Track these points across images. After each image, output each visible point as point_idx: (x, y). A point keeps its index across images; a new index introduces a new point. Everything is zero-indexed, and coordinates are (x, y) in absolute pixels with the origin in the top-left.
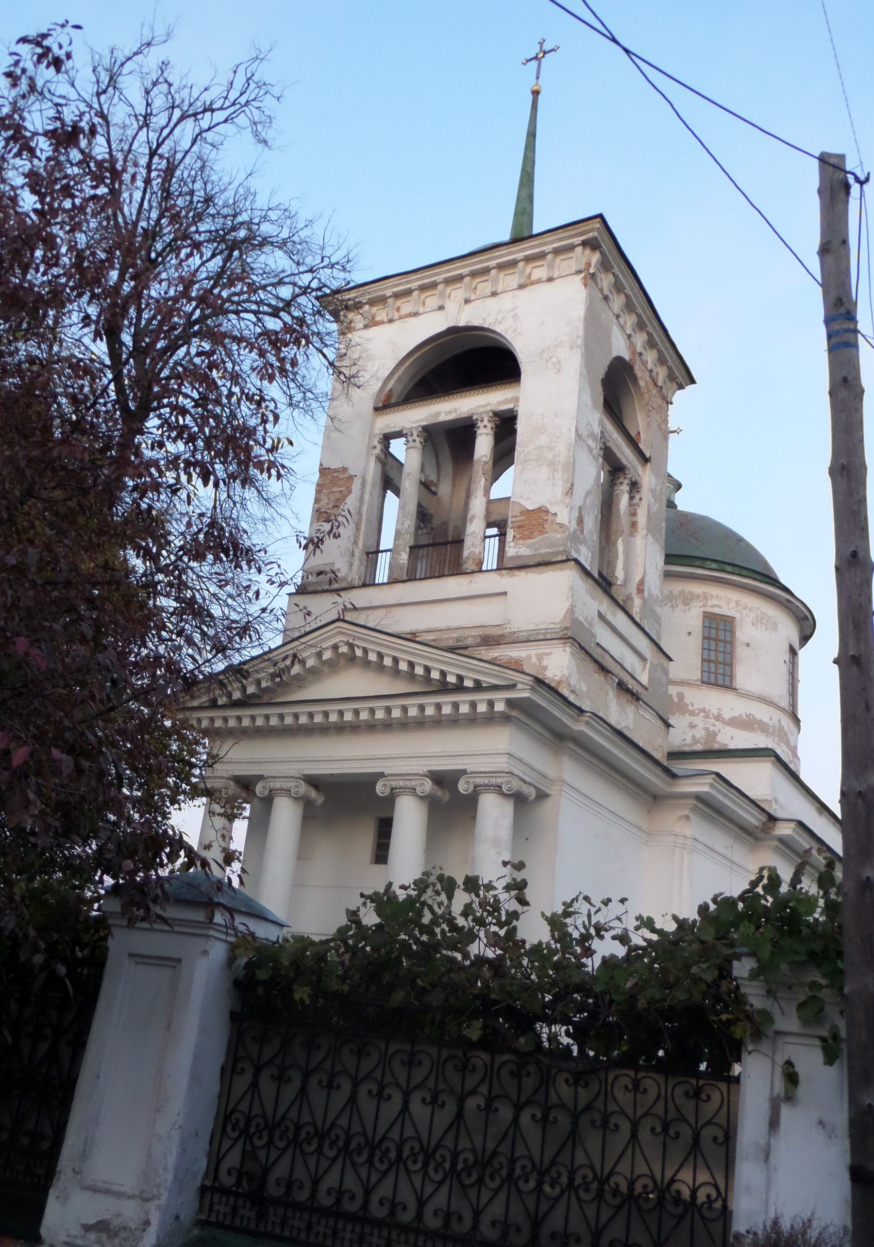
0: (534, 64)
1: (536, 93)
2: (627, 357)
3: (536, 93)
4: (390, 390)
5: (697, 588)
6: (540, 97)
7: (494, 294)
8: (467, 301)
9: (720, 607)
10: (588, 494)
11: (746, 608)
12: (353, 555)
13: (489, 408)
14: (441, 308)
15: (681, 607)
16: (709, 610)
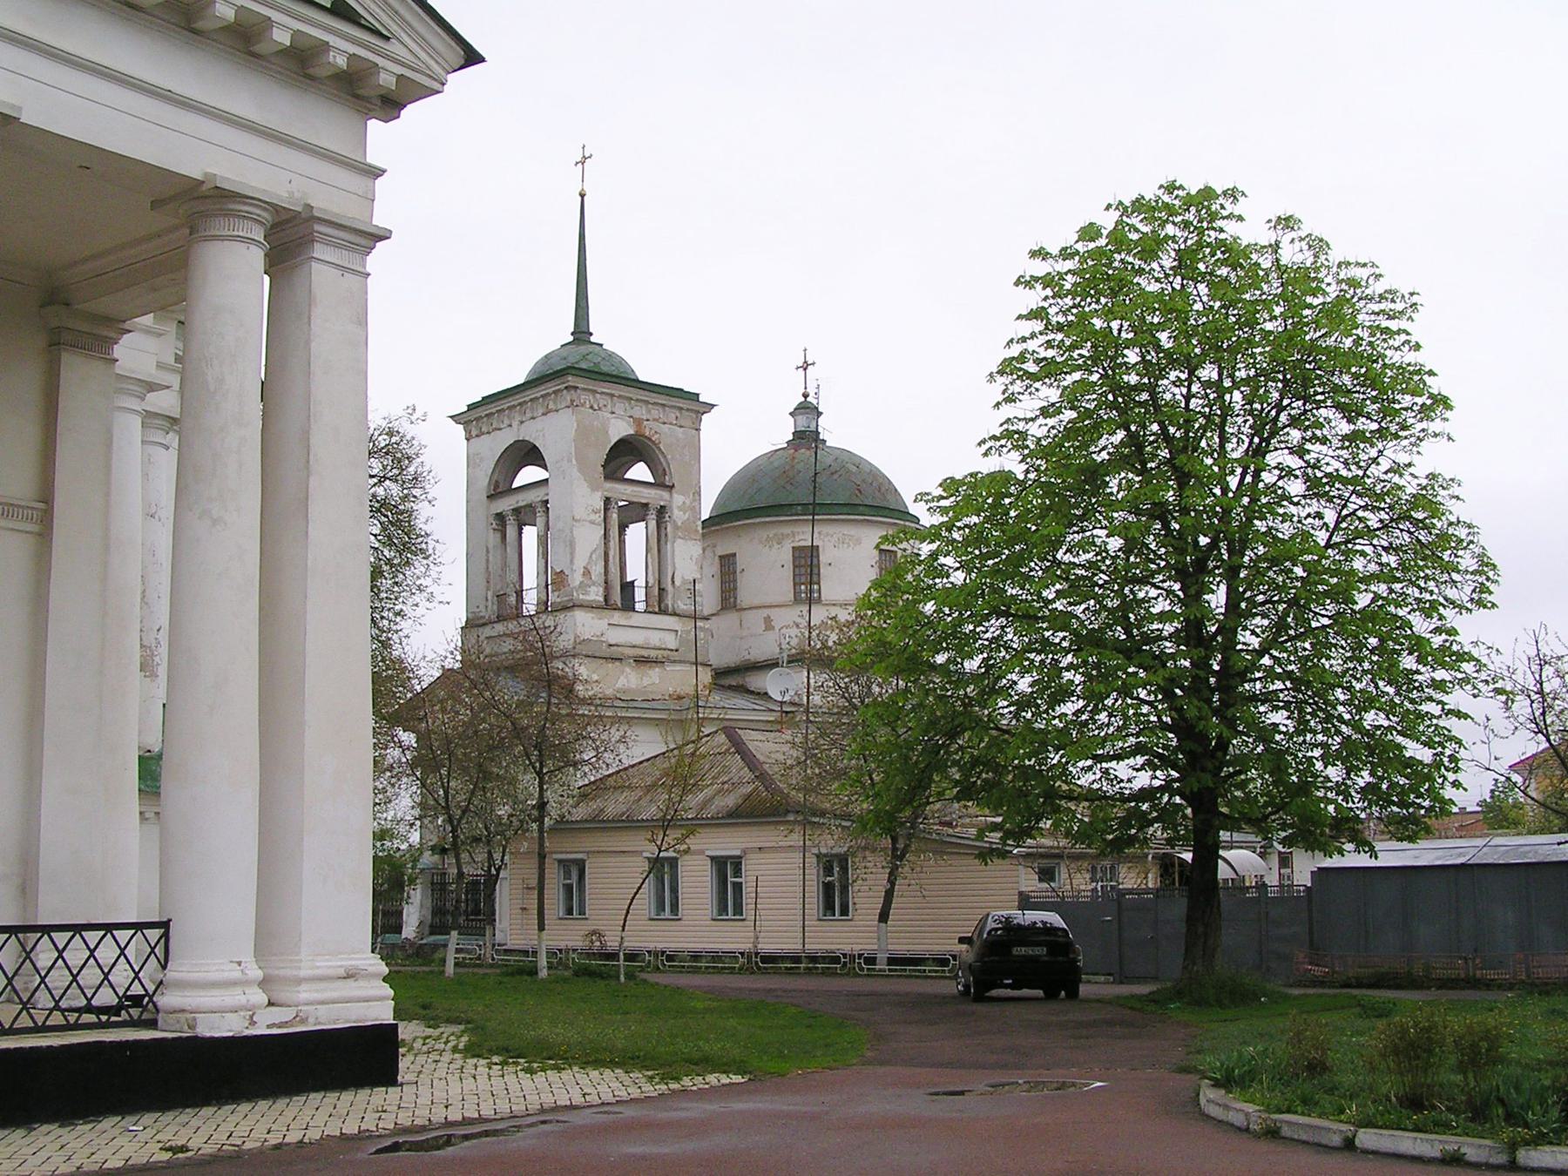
0: (580, 165)
1: (582, 196)
3: (582, 196)
4: (497, 481)
5: (787, 530)
6: (585, 198)
7: (533, 418)
8: (522, 422)
9: (805, 540)
10: (595, 551)
11: (828, 534)
12: (487, 600)
13: (539, 499)
14: (510, 426)
15: (776, 546)
16: (796, 544)
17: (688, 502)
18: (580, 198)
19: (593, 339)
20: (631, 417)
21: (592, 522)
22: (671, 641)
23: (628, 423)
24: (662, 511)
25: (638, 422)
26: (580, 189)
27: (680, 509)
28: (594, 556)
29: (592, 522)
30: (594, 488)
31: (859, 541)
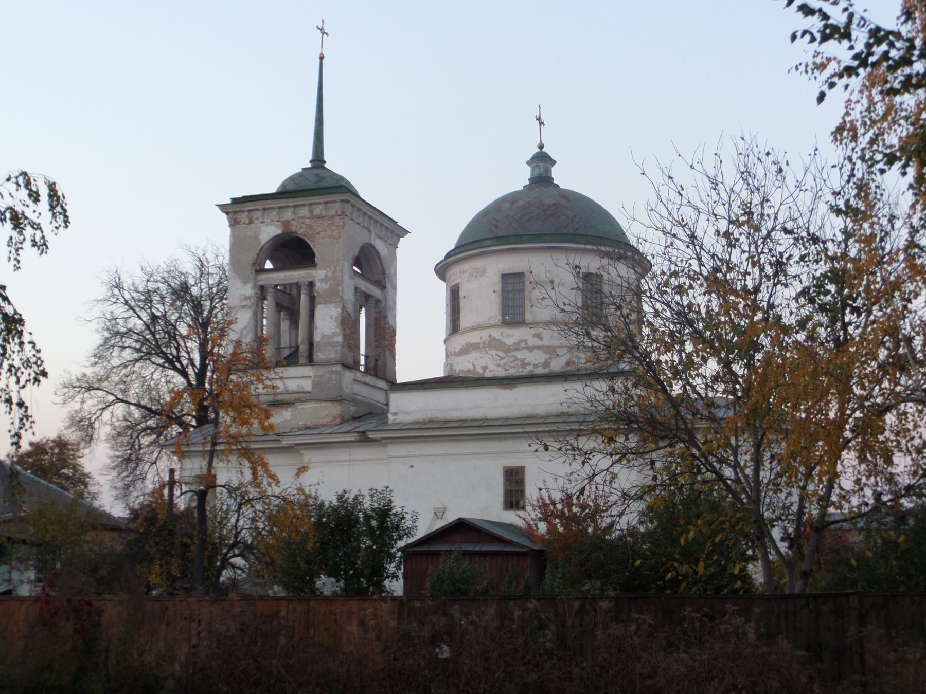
1: (322, 58)
2: (279, 232)
3: (322, 58)
10: (245, 328)
17: (329, 274)
18: (319, 60)
19: (326, 165)
20: (278, 221)
21: (244, 307)
22: (307, 385)
23: (277, 227)
24: (311, 284)
25: (286, 224)
26: (320, 52)
27: (321, 281)
28: (245, 332)
29: (244, 307)
30: (245, 282)
31: (484, 272)
